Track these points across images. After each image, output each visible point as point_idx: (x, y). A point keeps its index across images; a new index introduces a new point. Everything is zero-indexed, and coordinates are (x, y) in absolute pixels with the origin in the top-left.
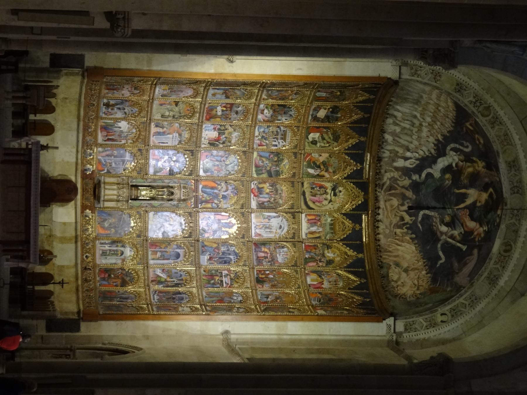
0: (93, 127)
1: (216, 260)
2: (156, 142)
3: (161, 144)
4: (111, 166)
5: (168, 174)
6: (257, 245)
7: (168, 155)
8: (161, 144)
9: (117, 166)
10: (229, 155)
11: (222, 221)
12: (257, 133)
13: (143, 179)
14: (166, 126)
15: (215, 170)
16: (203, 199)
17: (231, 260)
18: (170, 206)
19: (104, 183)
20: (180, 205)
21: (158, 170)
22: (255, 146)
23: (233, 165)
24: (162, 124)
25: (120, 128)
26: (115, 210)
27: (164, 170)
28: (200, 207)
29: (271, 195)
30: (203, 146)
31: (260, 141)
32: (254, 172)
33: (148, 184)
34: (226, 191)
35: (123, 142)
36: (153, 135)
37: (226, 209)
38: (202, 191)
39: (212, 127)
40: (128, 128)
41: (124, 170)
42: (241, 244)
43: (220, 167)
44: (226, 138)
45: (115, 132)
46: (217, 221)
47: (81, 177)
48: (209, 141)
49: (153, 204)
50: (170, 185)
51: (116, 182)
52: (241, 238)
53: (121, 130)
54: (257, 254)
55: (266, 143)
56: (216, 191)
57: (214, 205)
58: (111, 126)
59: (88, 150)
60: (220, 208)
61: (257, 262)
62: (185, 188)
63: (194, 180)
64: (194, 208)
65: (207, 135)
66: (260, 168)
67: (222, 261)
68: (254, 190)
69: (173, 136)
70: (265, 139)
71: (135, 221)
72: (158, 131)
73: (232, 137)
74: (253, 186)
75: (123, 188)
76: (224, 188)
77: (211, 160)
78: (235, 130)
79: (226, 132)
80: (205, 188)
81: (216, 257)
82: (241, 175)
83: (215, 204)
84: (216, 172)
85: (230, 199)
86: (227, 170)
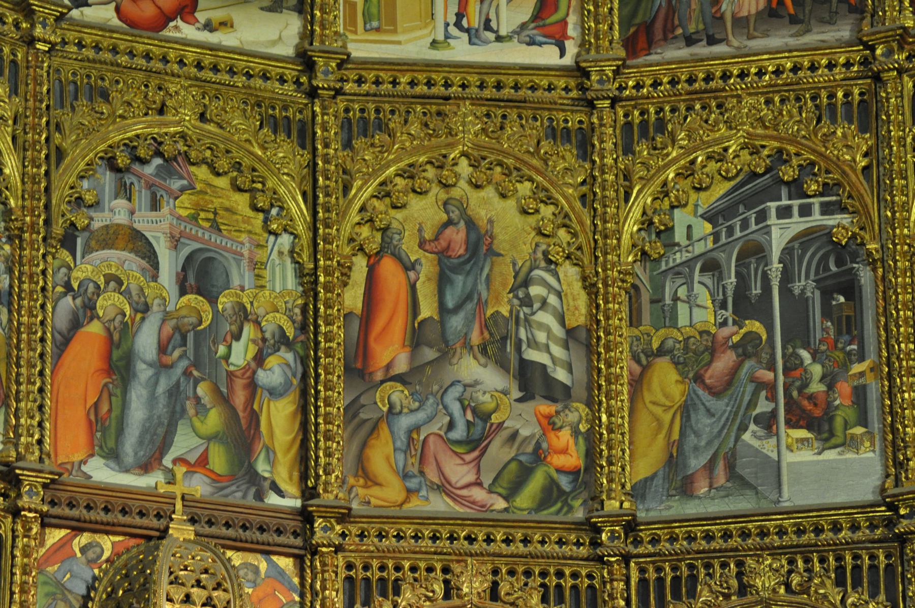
1: (817, 370)
6: (648, 28)
11: (427, 310)
16: (219, 461)
17: (805, 239)
34: (150, 256)
38: (145, 468)
42: (643, 149)
46: (429, 354)
52: (585, 149)
54: (740, 23)
60: (303, 328)
61: (830, 21)
63: (46, 522)
67: (827, 313)
80: (120, 430)
81: (792, 365)
83: (260, 359)
85: (216, 227)
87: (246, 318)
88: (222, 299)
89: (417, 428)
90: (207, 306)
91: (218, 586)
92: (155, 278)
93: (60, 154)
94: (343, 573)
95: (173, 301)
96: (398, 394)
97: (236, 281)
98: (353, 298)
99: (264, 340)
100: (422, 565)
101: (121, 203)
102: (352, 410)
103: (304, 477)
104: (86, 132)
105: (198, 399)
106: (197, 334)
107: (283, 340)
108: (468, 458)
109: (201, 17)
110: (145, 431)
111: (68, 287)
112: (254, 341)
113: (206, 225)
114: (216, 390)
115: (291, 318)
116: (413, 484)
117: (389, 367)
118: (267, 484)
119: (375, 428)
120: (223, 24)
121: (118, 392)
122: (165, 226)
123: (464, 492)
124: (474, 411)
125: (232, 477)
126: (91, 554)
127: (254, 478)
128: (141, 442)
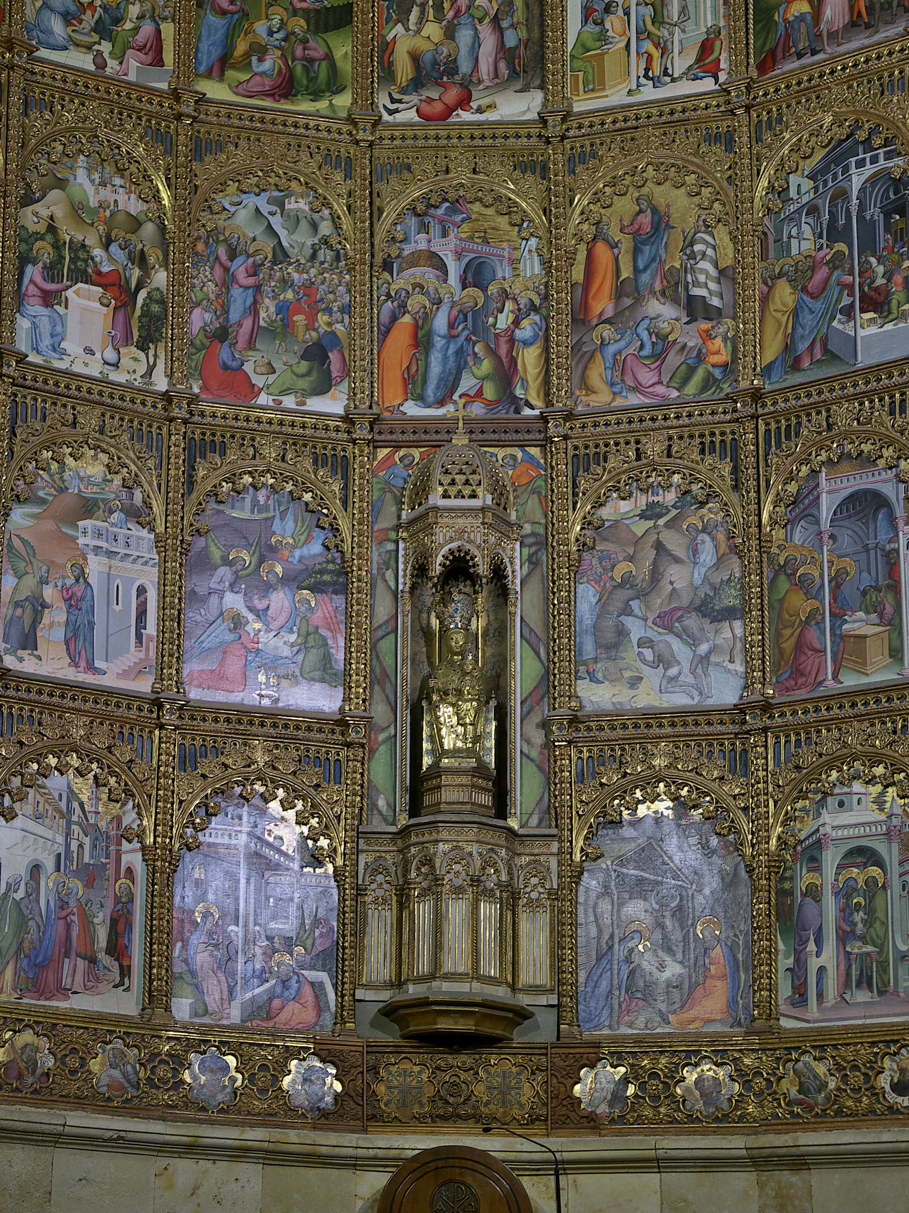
0: (28, 1037)
2: (133, 655)
3: (151, 629)
4: (289, 943)
5: (339, 600)
7: (221, 595)
8: (151, 629)
9: (293, 910)
10: (214, 234)
12: (84, 61)
13: (372, 752)
14: (30, 582)
15: (311, 326)
16: (490, 392)
18: (535, 585)
19: (398, 983)
20: (528, 529)
21: (314, 655)
22: (164, 86)
23: (277, 222)
24: (17, 604)
25: (36, 869)
26: (574, 914)
27: (317, 618)
28: (537, 412)
29: (457, 14)
30: (161, 384)
31: (130, 52)
32: (322, 105)
33: (404, 716)
34: (442, 267)
35: (132, 857)
36: (91, 668)
37: (547, 265)
38: (441, 403)
39: (35, 308)
40: (38, 817)
41: (316, 860)
43: (290, 295)
44: (107, 243)
45: (63, 905)
47: (366, 1131)
48: (127, 340)
49: (530, 685)
50: (404, 583)
51: (389, 915)
53: (49, 864)
55: (141, 17)
56: (440, 323)
57: (526, 331)
58: (22, 923)
59: (187, 1077)
60: (546, 297)
62: (422, 490)
63: (375, 445)
64: (545, 443)
65: (90, 351)
66: (299, 69)
68: (425, 108)
69: (97, 549)
70: (118, 21)
71: (638, 794)
72: (59, 634)
73: (102, 205)
74: (410, 115)
75: (428, 861)
76: (426, 274)
77: (251, 344)
78: (61, 184)
79: (68, 232)
80: (425, 382)
82: (338, 177)
83: (516, 323)
84: (322, 318)
85: (486, 241)
86: (314, 256)
87: (507, 297)
88: (490, 288)
89: (620, 352)
90: (481, 294)
91: (474, 472)
92: (445, 281)
93: (381, 211)
94: (571, 452)
95: (458, 294)
96: (607, 332)
97: (500, 275)
98: (578, 273)
99: (519, 310)
100: (622, 441)
101: (423, 235)
102: (576, 347)
103: (547, 394)
104: (397, 195)
105: (475, 354)
106: (476, 314)
107: (533, 308)
108: (653, 366)
109: (475, 105)
110: (441, 379)
111: (389, 296)
112: (512, 312)
113: (480, 241)
114: (488, 347)
115: (537, 292)
116: (617, 389)
117: (601, 314)
118: (522, 402)
119: (592, 356)
120: (489, 107)
121: (422, 357)
122: (452, 246)
123: (650, 390)
124: (657, 336)
125: (498, 402)
126: (406, 462)
127: (514, 400)
128: (438, 387)
